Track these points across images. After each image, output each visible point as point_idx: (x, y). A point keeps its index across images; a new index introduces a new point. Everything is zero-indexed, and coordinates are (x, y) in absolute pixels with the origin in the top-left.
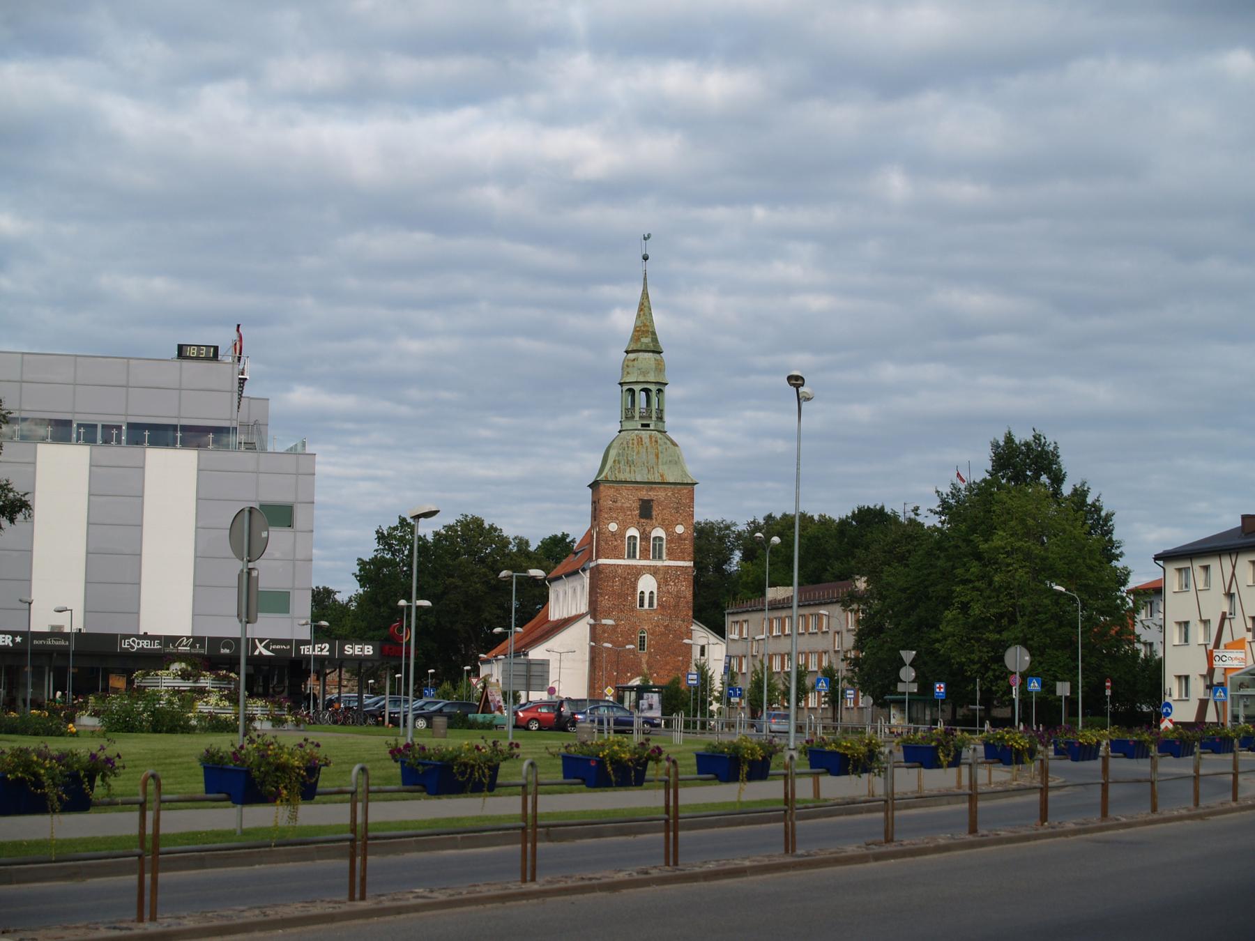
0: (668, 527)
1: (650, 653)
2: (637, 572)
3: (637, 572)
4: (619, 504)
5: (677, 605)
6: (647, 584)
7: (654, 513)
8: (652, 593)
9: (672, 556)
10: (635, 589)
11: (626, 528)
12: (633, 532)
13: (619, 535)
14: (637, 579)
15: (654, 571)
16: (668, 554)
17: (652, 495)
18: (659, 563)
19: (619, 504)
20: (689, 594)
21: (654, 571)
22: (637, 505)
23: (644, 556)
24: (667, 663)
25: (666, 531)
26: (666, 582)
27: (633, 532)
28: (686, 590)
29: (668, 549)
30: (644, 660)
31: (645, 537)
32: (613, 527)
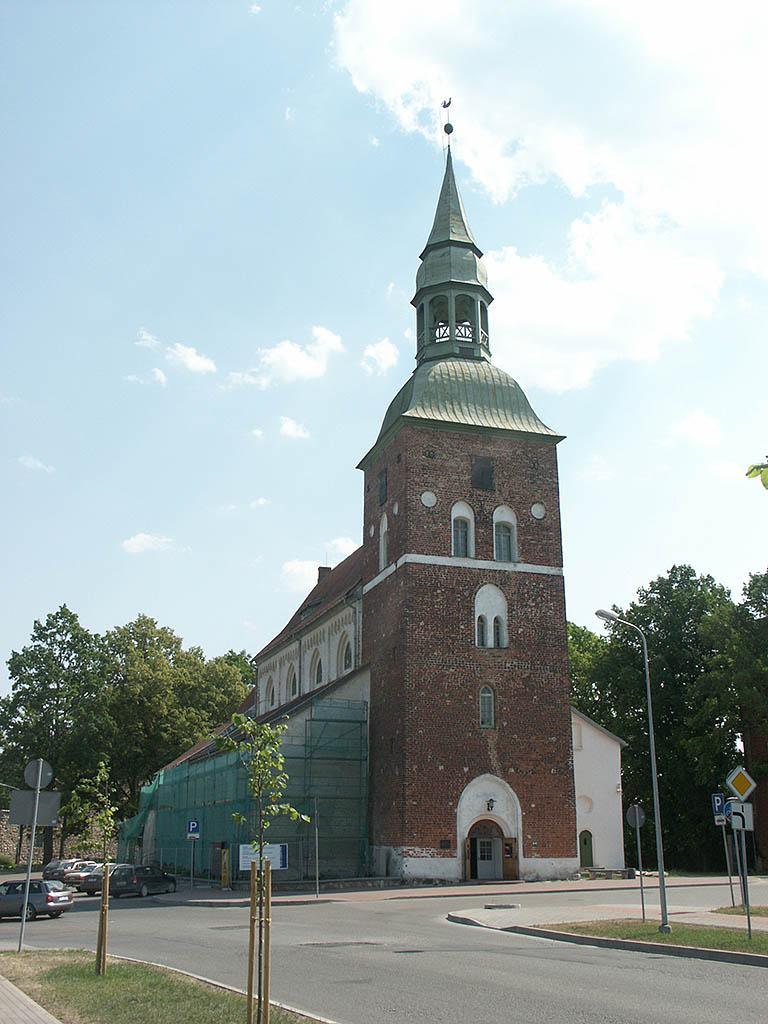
0: (520, 507)
2: (475, 580)
3: (475, 580)
6: (490, 603)
7: (496, 481)
8: (496, 620)
11: (450, 504)
12: (461, 511)
15: (501, 580)
16: (522, 553)
17: (491, 450)
18: (509, 567)
21: (501, 580)
23: (484, 552)
25: (518, 512)
27: (461, 511)
29: (523, 543)
30: (491, 743)
31: (483, 520)
32: (429, 499)
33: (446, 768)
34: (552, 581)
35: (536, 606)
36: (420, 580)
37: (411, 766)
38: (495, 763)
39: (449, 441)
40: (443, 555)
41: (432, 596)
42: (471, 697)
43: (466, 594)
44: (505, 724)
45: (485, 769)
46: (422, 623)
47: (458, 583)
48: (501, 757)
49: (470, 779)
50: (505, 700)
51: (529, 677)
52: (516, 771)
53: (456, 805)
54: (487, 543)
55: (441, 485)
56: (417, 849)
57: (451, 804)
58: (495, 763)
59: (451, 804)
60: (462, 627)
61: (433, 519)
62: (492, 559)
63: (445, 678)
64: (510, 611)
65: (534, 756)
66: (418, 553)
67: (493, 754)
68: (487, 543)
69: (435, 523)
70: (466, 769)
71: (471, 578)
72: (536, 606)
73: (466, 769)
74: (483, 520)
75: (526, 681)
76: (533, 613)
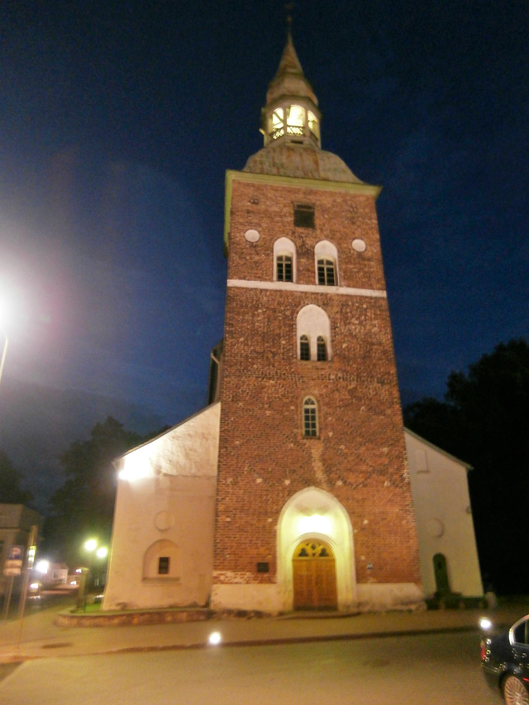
0: (341, 241)
1: (327, 440)
4: (262, 207)
5: (367, 356)
7: (318, 222)
9: (351, 280)
10: (292, 327)
11: (273, 239)
13: (266, 247)
14: (295, 312)
15: (324, 302)
19: (262, 207)
20: (385, 338)
22: (289, 210)
24: (360, 460)
26: (346, 321)
28: (381, 332)
31: (305, 252)
32: (252, 235)
33: (265, 480)
34: (375, 302)
35: (361, 323)
36: (241, 301)
37: (225, 479)
38: (320, 475)
39: (273, 192)
40: (265, 280)
41: (253, 315)
42: (292, 408)
43: (288, 313)
44: (331, 434)
45: (309, 482)
46: (242, 339)
47: (279, 304)
48: (328, 469)
49: (291, 492)
50: (331, 411)
51: (356, 388)
52: (345, 483)
53: (275, 522)
54: (308, 270)
55: (264, 225)
56: (230, 574)
57: (270, 520)
58: (320, 475)
59: (270, 520)
60: (284, 342)
61: (256, 251)
62: (314, 283)
63: (265, 390)
64: (334, 327)
65: (364, 468)
66: (240, 278)
67: (317, 466)
68: (308, 270)
69: (257, 254)
70: (287, 482)
71: (293, 299)
72: (361, 323)
73: (287, 482)
74: (305, 252)
75: (352, 392)
76: (355, 327)
